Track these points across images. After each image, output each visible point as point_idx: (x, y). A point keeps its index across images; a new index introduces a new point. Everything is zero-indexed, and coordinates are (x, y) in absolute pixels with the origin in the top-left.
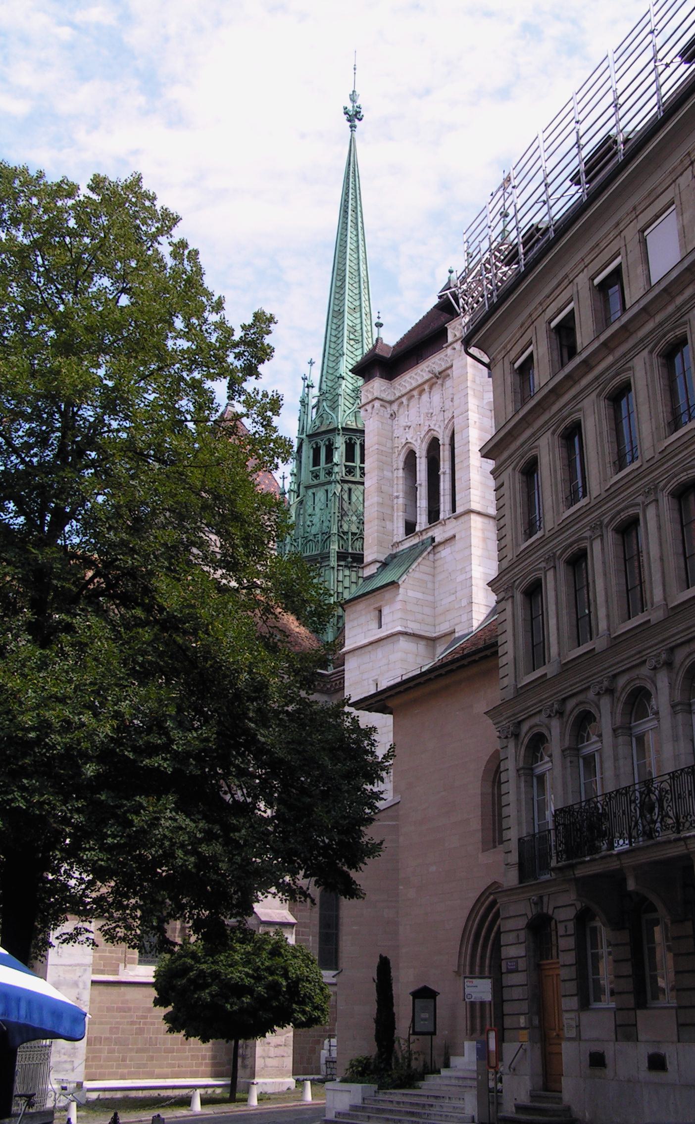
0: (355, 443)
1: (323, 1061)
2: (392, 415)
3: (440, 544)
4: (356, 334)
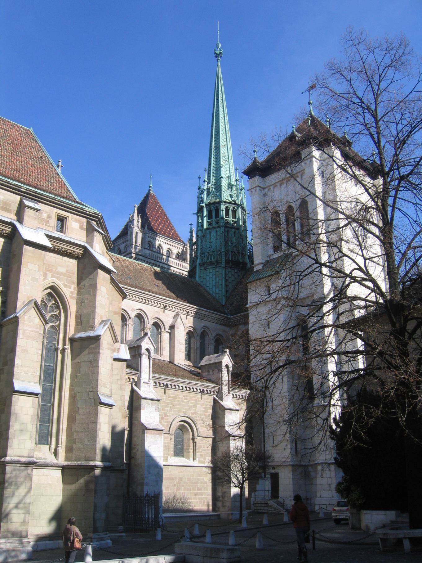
1: (252, 503)
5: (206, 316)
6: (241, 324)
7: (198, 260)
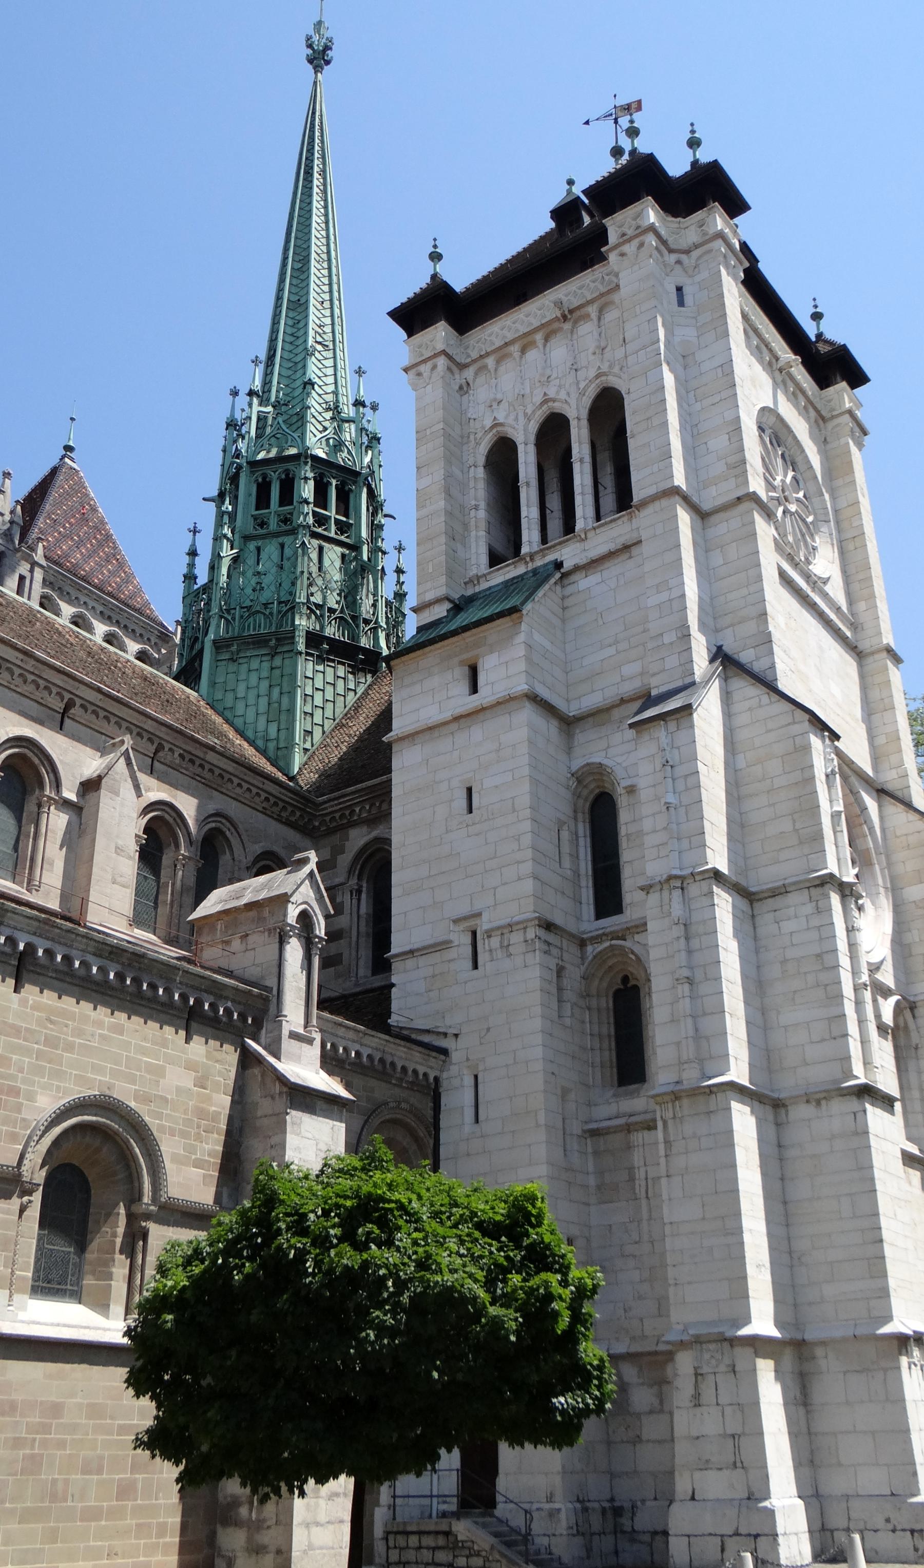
2: (461, 388)
3: (577, 569)
4: (324, 336)
5: (227, 776)
6: (353, 824)
7: (212, 629)
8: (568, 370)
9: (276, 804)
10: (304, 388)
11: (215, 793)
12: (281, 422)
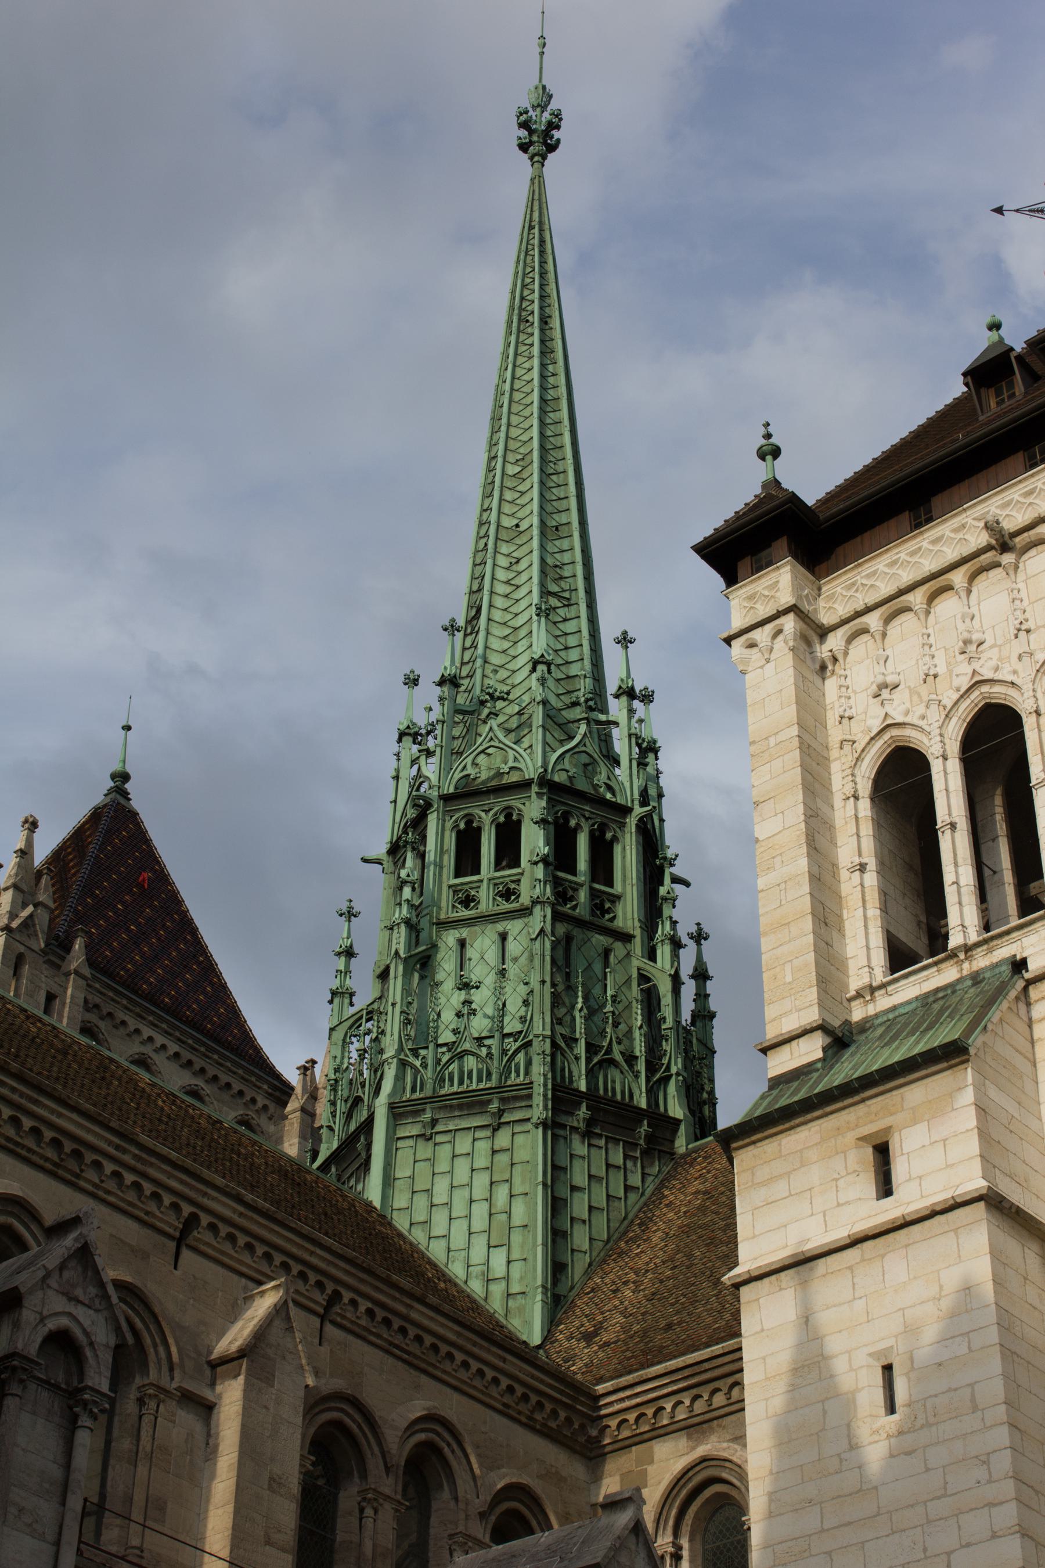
0: (578, 826)
5: (444, 1348)
6: (658, 1433)
7: (387, 1086)
8: (1014, 631)
9: (525, 1398)
10: (534, 670)
11: (424, 1379)
12: (495, 728)
